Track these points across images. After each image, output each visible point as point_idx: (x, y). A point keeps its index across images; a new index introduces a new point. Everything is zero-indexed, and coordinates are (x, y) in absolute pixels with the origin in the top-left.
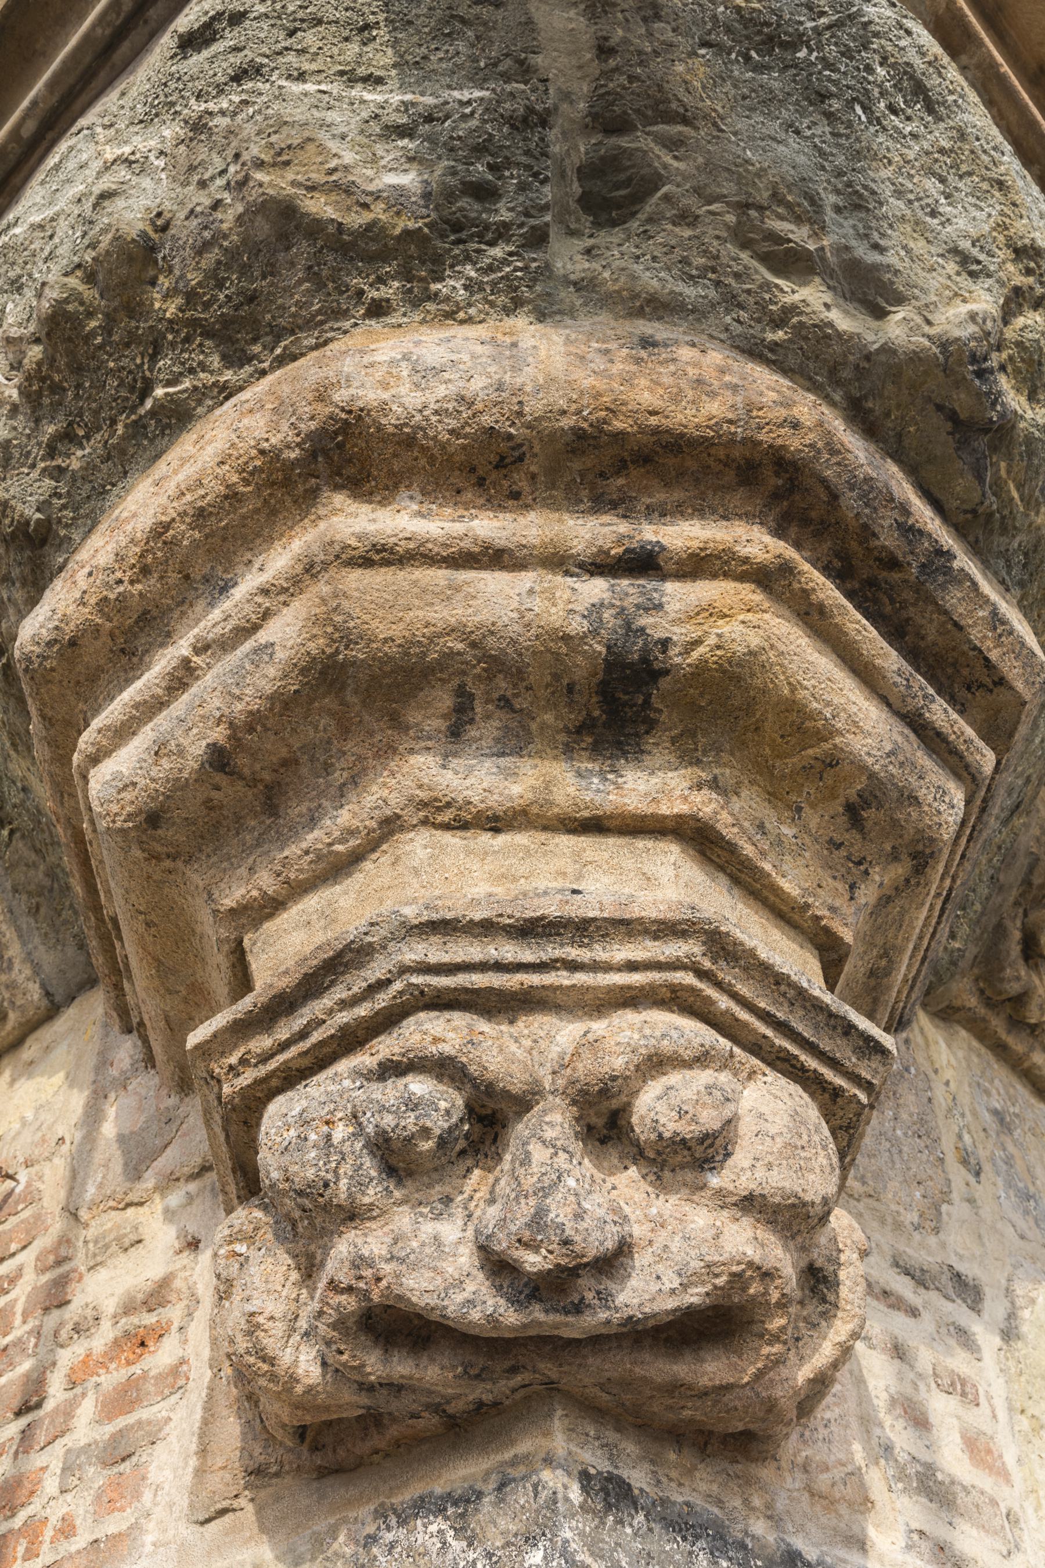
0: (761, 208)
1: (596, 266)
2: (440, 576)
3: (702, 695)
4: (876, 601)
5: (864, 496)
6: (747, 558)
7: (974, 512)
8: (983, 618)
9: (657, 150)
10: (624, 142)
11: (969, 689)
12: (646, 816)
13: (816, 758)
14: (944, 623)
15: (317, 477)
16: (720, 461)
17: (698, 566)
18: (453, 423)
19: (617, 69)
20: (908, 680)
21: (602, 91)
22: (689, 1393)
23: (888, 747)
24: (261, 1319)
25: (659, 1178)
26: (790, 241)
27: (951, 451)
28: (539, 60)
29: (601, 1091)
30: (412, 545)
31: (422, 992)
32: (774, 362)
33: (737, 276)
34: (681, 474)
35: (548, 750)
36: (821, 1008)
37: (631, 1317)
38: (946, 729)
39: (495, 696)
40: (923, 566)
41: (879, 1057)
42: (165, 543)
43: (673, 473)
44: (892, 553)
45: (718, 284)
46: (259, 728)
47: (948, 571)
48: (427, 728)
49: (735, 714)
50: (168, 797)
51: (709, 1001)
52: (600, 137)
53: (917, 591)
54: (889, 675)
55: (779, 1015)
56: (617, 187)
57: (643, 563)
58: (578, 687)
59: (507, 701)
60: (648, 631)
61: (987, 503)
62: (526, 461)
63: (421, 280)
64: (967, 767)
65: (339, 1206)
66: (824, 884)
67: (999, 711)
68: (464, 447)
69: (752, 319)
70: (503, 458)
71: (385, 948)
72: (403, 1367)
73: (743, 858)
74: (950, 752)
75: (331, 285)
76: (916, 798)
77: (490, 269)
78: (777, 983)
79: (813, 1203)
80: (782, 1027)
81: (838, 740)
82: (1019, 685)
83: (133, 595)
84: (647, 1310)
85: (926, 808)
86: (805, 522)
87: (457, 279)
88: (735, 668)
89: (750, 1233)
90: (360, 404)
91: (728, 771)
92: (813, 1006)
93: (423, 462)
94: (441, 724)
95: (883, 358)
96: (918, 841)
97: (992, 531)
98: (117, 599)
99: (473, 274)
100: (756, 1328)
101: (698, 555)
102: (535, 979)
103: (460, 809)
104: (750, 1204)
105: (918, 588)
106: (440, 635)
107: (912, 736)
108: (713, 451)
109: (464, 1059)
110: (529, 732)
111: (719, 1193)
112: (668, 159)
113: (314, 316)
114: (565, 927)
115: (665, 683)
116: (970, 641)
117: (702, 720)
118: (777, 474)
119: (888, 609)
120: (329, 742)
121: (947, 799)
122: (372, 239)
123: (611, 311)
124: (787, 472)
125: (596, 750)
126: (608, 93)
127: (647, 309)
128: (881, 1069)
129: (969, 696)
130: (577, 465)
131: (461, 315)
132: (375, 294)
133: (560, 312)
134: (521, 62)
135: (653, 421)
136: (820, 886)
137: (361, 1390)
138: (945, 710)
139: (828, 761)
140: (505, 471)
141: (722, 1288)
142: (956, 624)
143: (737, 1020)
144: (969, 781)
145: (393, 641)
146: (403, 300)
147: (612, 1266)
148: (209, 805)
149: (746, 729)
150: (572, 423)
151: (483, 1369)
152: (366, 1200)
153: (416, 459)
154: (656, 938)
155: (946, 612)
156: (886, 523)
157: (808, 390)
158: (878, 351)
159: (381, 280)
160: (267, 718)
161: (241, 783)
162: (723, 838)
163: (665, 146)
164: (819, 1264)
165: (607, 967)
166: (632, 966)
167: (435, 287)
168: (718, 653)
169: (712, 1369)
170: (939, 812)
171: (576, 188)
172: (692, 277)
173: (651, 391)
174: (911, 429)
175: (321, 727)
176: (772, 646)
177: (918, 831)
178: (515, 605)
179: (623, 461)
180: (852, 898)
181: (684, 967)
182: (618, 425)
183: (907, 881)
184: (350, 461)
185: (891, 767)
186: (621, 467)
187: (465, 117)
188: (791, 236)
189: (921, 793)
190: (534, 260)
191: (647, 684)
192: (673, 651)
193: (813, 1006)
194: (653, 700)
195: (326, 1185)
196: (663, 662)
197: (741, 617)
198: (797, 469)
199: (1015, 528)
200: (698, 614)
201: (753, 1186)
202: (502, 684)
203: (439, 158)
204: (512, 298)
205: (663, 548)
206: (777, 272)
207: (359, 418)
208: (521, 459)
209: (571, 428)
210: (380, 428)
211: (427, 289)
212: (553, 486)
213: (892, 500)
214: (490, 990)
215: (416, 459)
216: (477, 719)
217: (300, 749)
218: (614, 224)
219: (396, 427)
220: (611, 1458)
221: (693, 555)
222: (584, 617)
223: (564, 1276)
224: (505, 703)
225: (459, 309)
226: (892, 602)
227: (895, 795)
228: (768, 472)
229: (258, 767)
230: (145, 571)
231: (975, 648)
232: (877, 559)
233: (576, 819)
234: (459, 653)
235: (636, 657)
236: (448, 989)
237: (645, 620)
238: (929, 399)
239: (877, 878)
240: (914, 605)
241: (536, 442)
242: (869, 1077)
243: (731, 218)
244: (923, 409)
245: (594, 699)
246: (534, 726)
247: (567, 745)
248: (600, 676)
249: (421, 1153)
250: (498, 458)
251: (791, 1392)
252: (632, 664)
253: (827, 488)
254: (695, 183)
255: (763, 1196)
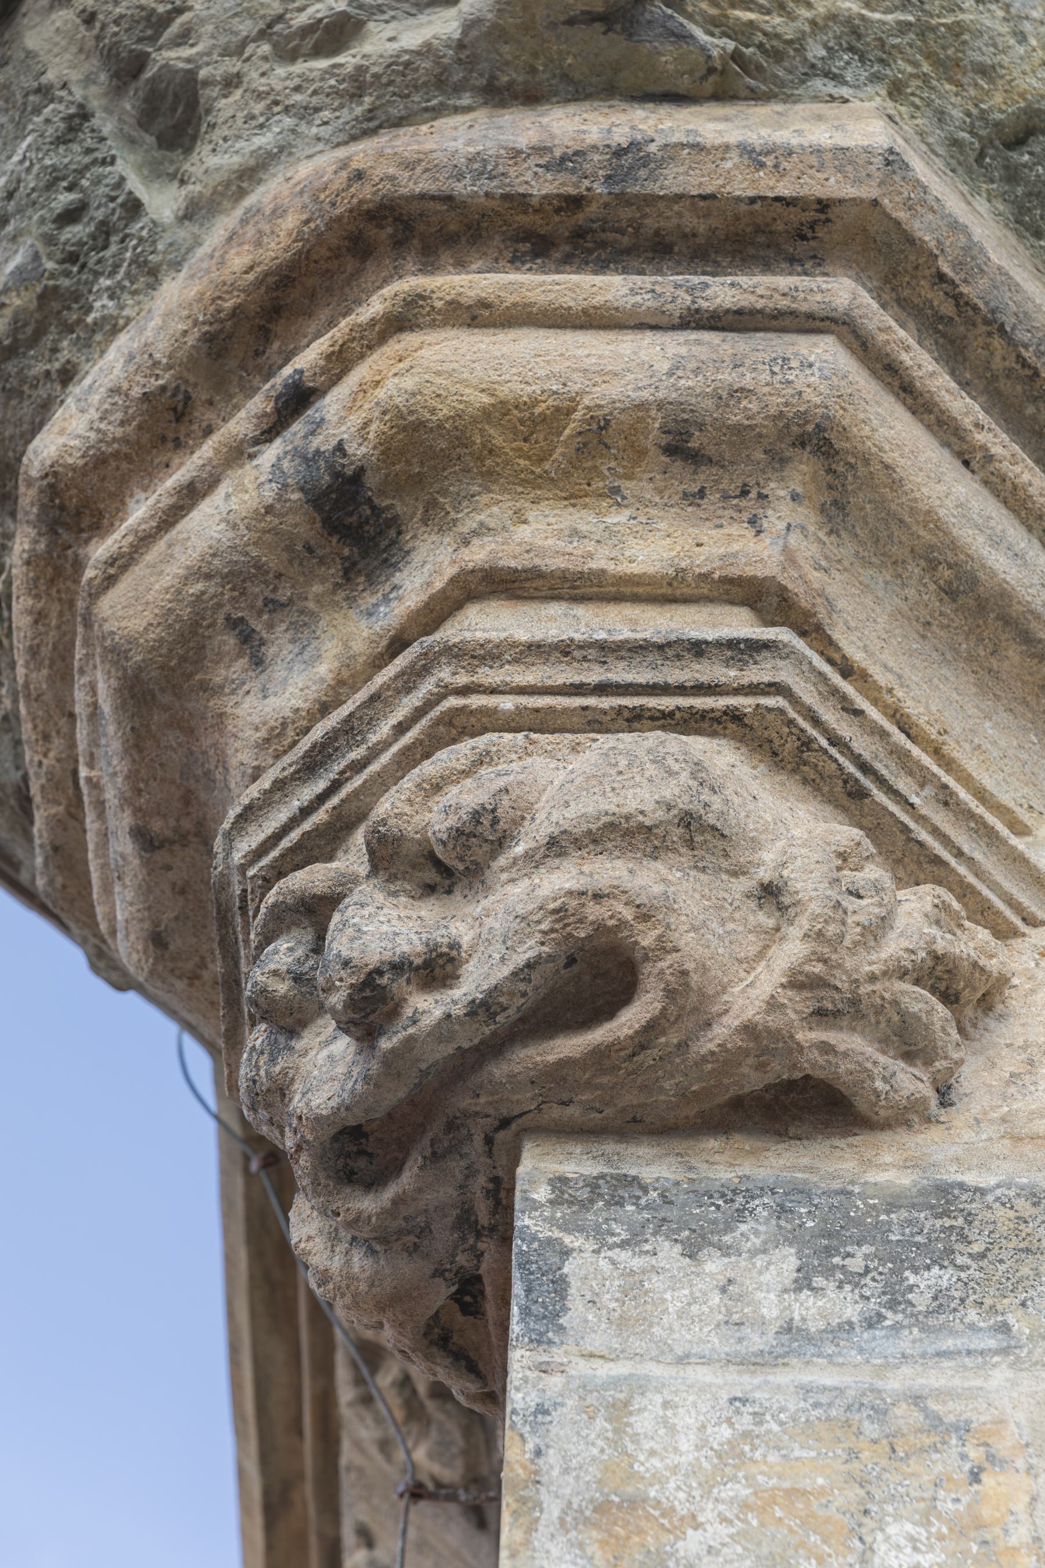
0: (280, 18)
1: (190, 187)
2: (160, 546)
3: (408, 463)
4: (603, 244)
5: (482, 173)
6: (373, 319)
7: (711, 70)
8: (736, 167)
9: (172, 54)
10: (148, 74)
11: (803, 238)
12: (427, 604)
13: (580, 433)
14: (693, 204)
15: (70, 547)
16: (329, 258)
17: (340, 363)
18: (119, 416)
19: (103, 27)
20: (653, 291)
21: (105, 52)
22: (622, 1053)
23: (666, 366)
24: (302, 1245)
25: (483, 882)
26: (321, 20)
27: (625, 44)
28: (50, 76)
29: (379, 840)
30: (130, 538)
31: (264, 879)
32: (380, 127)
33: (297, 89)
34: (313, 296)
35: (336, 615)
36: (641, 647)
37: (473, 1001)
38: (745, 301)
39: (260, 603)
40: (608, 177)
41: (765, 653)
42: (36, 700)
43: (306, 301)
44: (558, 195)
45: (287, 110)
46: (142, 786)
47: (646, 161)
48: (235, 676)
49: (454, 455)
50: (149, 908)
51: (484, 711)
52: (133, 85)
53: (629, 203)
54: (620, 303)
55: (588, 681)
56: (174, 110)
57: (298, 399)
58: (312, 542)
59: (273, 601)
60: (322, 449)
61: (715, 53)
62: (194, 396)
63: (80, 321)
64: (810, 316)
65: (268, 1090)
66: (705, 539)
67: (865, 230)
68: (140, 427)
69: (335, 110)
70: (175, 409)
71: (228, 868)
72: (390, 1192)
73: (559, 573)
74: (775, 318)
75: (26, 388)
76: (742, 390)
77: (116, 267)
78: (566, 654)
79: (642, 812)
80: (602, 689)
81: (587, 401)
82: (850, 191)
83: (53, 767)
84: (485, 987)
85: (766, 390)
86: (450, 240)
87: (100, 298)
88: (410, 418)
89: (575, 872)
90: (48, 462)
91: (495, 509)
92: (630, 650)
93: (125, 466)
94: (243, 662)
95: (474, 33)
96: (787, 426)
97: (759, 68)
98: (49, 780)
99: (108, 282)
100: (638, 955)
101: (333, 353)
102: (335, 801)
103: (294, 722)
104: (557, 846)
105: (623, 199)
106: (179, 592)
107: (707, 336)
108: (315, 257)
109: (281, 898)
110: (312, 614)
111: (528, 856)
112: (186, 52)
113: (33, 423)
114: (336, 740)
115: (371, 480)
116: (739, 199)
117: (431, 484)
118: (381, 227)
119: (626, 241)
120: (192, 753)
121: (794, 364)
122: (25, 325)
123: (221, 212)
124: (385, 217)
125: (371, 581)
126: (110, 50)
127: (244, 185)
128: (781, 663)
129: (812, 243)
130: (233, 363)
131: (121, 322)
132: (57, 365)
133: (190, 250)
134: (38, 90)
135: (251, 277)
136: (699, 545)
137: (410, 1255)
138: (732, 285)
139: (595, 426)
140: (186, 418)
141: (553, 930)
142: (704, 197)
143: (537, 710)
144: (833, 326)
145: (151, 625)
146: (79, 350)
147: (458, 977)
148: (182, 890)
149: (480, 459)
150: (197, 335)
151: (432, 1145)
152: (278, 1069)
153: (118, 468)
154: (408, 690)
155: (679, 197)
156: (528, 176)
157: (434, 119)
158: (465, 33)
159: (55, 350)
160: (138, 771)
161: (176, 847)
162: (516, 570)
163: (179, 45)
164: (766, 881)
165: (386, 745)
166: (401, 729)
167: (89, 319)
168: (387, 418)
169: (630, 1019)
170: (789, 382)
171: (150, 140)
172: (261, 126)
173: (238, 254)
174: (569, 61)
175: (175, 745)
176: (438, 373)
177: (775, 418)
178: (218, 518)
179: (261, 328)
180: (759, 532)
181: (441, 697)
182: (228, 305)
183: (830, 471)
184: (78, 514)
185: (682, 382)
186: (265, 334)
187: (28, 170)
188: (319, 15)
189: (747, 381)
190: (142, 228)
191: (358, 493)
192: (351, 448)
193: (630, 650)
194: (376, 501)
195: (254, 1082)
196: (352, 464)
197: (394, 371)
198: (392, 208)
199: (790, 42)
200: (355, 400)
201: (550, 830)
202: (255, 589)
203: (30, 218)
204: (148, 273)
205: (301, 372)
206: (335, 52)
207: (55, 473)
208: (188, 398)
209: (199, 340)
210: (74, 468)
211: (87, 325)
212: (231, 397)
213: (521, 152)
214: (306, 835)
215: (118, 468)
216: (265, 635)
217: (181, 777)
218: (194, 138)
219: (83, 456)
220: (609, 1162)
221: (329, 357)
222: (271, 481)
223: (368, 993)
224: (273, 606)
225: (117, 318)
226: (622, 232)
227: (709, 403)
228: (371, 231)
229: (172, 823)
230: (46, 737)
231: (753, 200)
232: (558, 211)
233: (382, 654)
234: (203, 593)
235: (327, 478)
236: (276, 860)
237: (316, 442)
238: (553, 25)
239: (782, 493)
240: (645, 216)
241: (185, 374)
242: (766, 679)
243: (266, 48)
244: (558, 37)
245: (334, 540)
246: (311, 605)
247: (347, 599)
248: (318, 519)
249: (285, 997)
250: (172, 413)
251: (764, 1006)
252: (329, 486)
253: (433, 198)
254: (219, 50)
255: (565, 832)
